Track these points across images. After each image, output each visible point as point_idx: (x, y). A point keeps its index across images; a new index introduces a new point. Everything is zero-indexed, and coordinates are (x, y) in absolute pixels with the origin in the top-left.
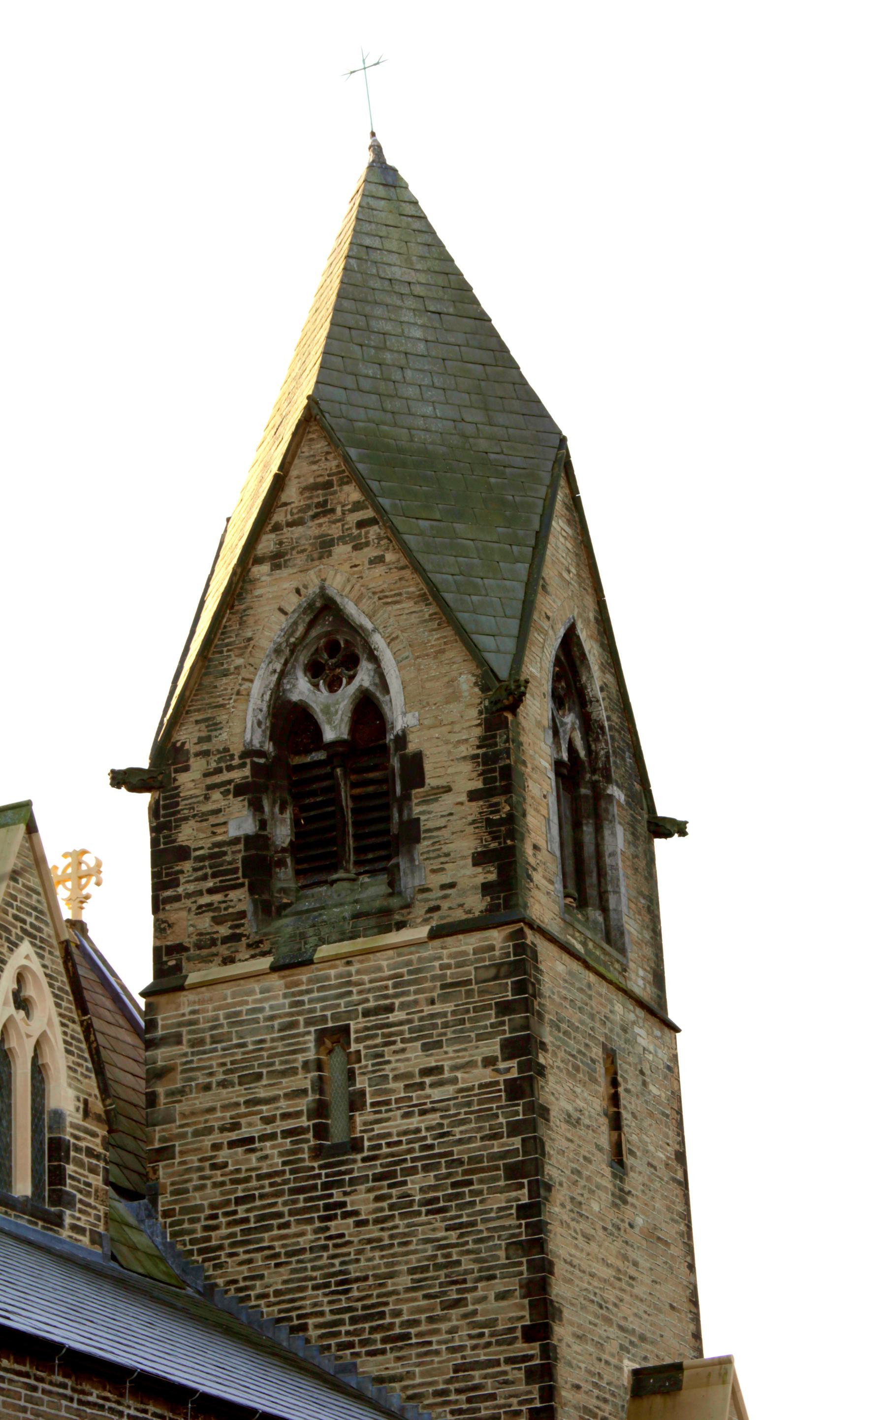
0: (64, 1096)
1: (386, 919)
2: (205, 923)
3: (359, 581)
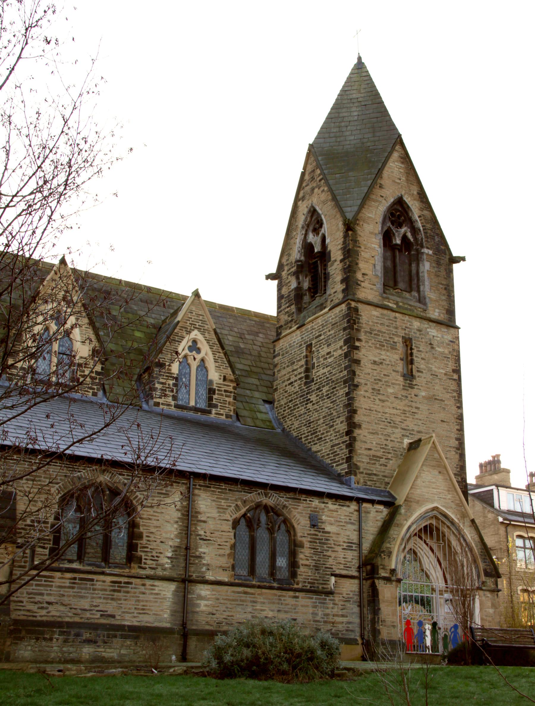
0: (214, 376)
1: (322, 307)
2: (286, 317)
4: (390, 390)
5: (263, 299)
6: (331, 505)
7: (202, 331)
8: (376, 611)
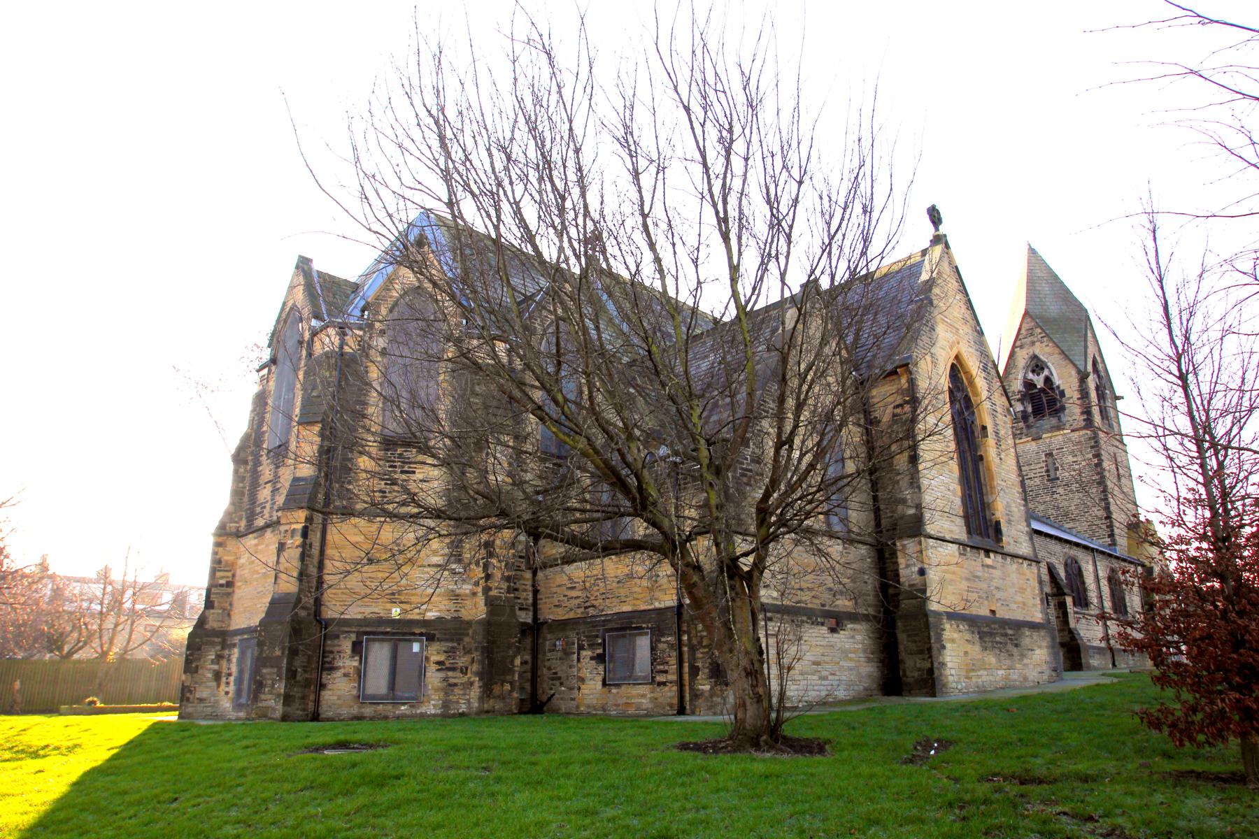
1: (1059, 428)
3: (1043, 351)
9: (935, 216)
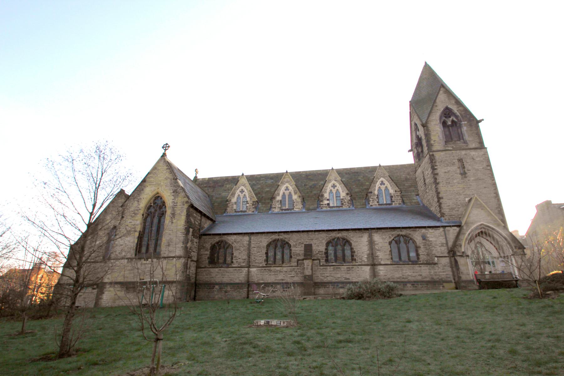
0: (392, 191)
4: (455, 181)
5: (409, 159)
6: (430, 230)
7: (384, 177)
8: (458, 269)
9: (166, 147)
